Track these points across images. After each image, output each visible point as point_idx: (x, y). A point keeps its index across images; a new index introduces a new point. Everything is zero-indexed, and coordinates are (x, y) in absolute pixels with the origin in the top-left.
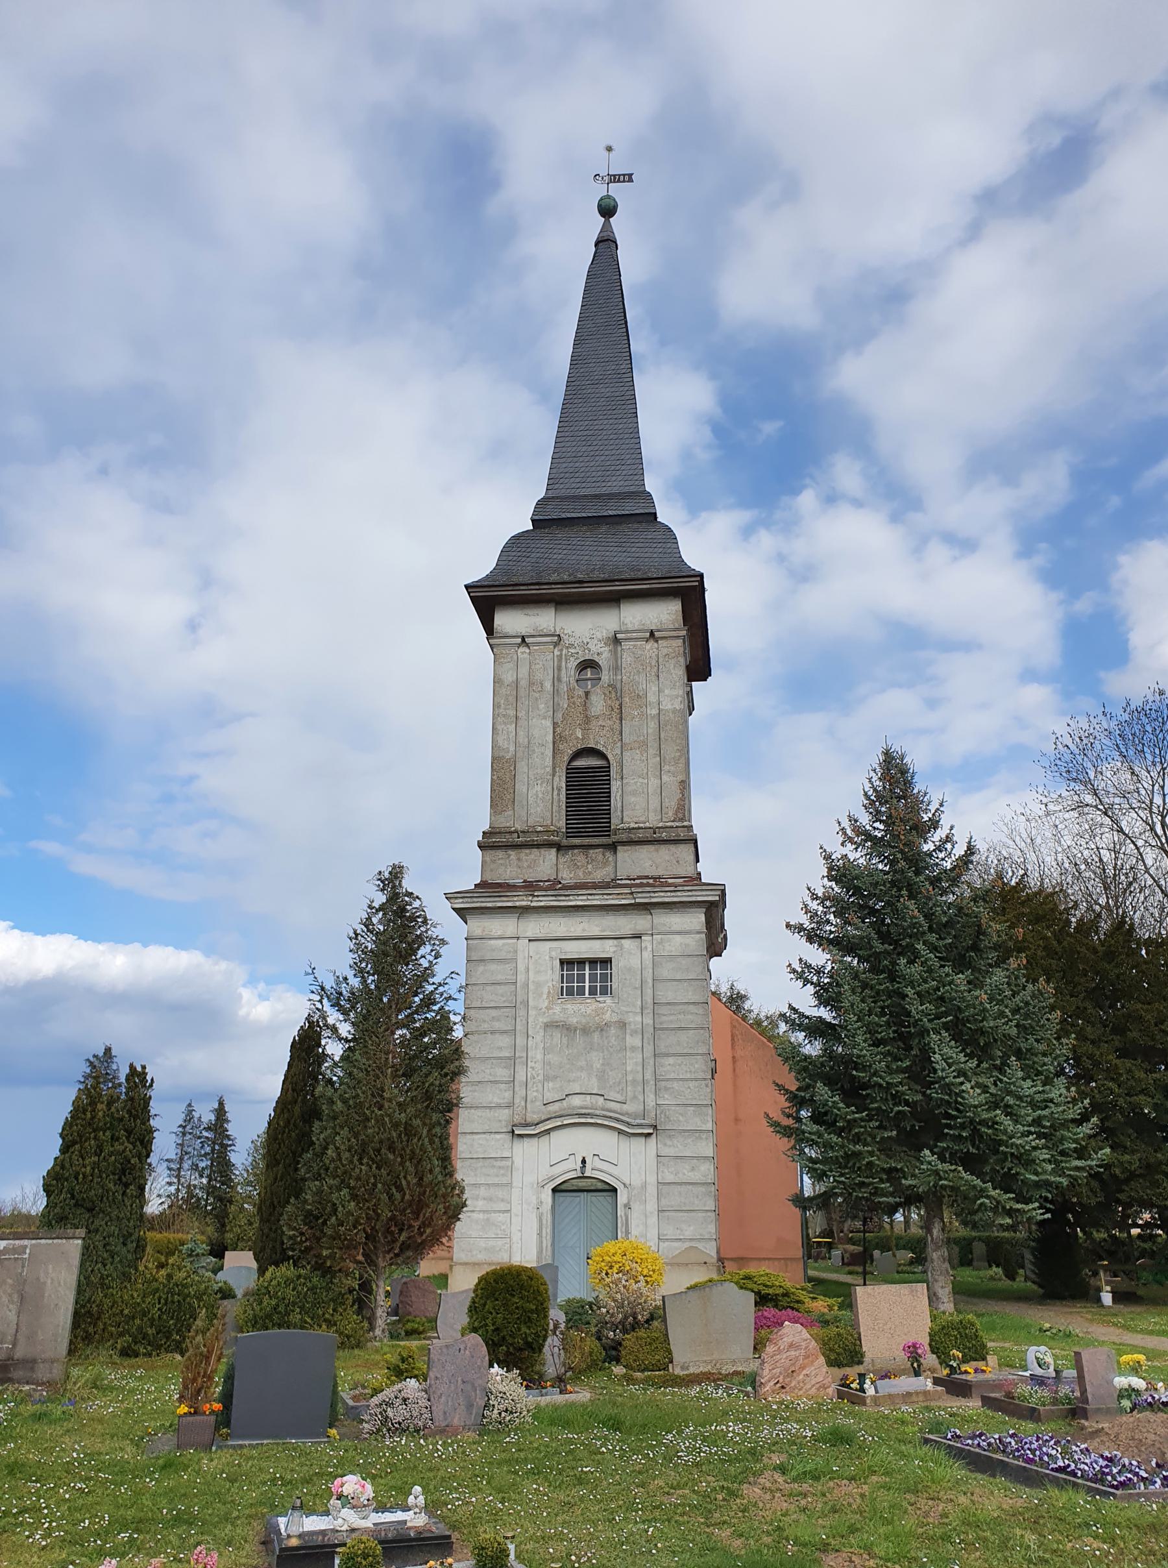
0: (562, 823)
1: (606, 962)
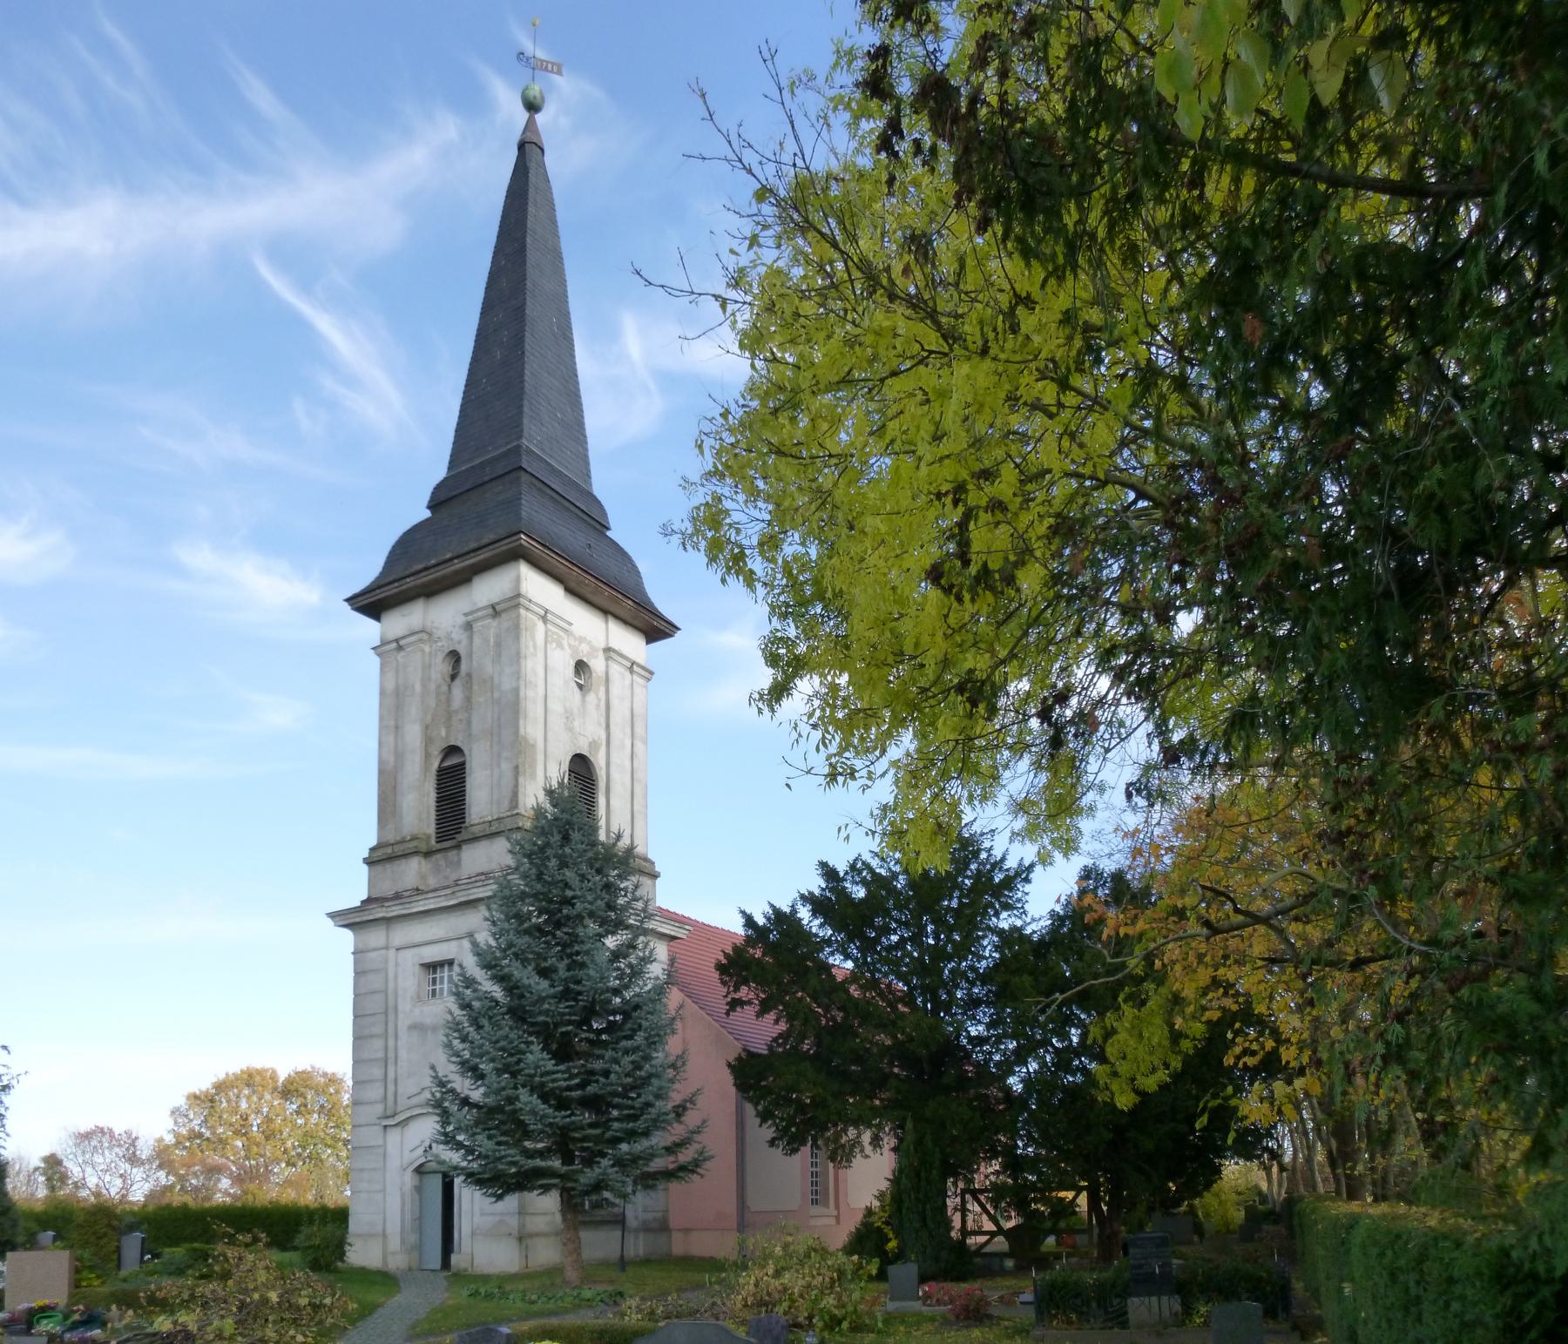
0: (430, 828)
1: (450, 963)
